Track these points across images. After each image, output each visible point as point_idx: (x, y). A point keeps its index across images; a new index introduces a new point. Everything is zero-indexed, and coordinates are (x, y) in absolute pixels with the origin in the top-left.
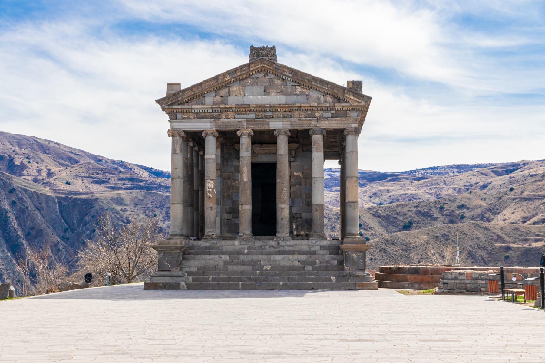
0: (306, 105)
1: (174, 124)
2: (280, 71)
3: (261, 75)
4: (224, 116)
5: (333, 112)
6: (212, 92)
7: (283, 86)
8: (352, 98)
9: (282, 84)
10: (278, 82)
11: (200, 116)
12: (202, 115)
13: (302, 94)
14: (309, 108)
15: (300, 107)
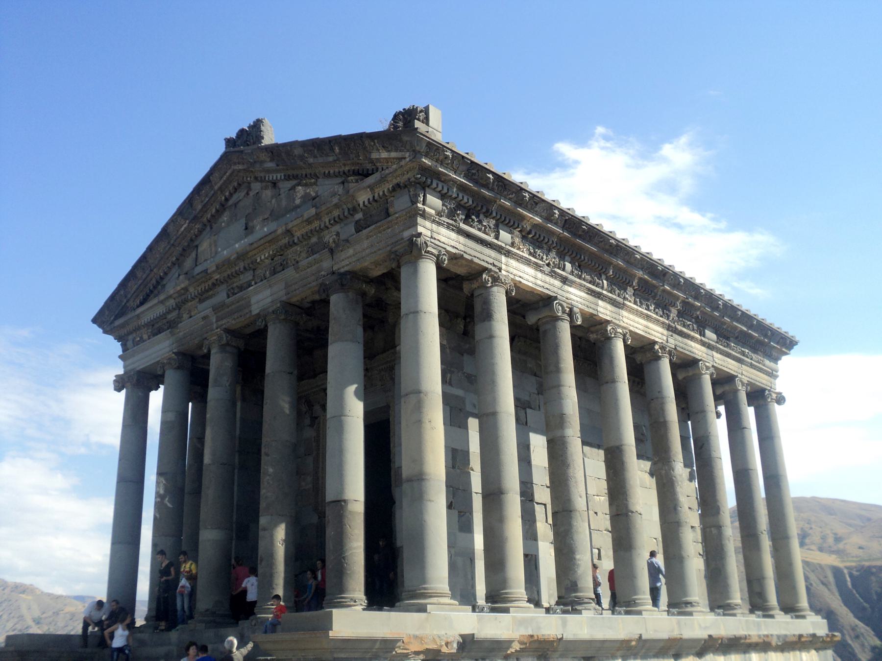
0: (295, 223)
1: (129, 362)
2: (258, 165)
3: (241, 194)
4: (185, 316)
5: (359, 216)
6: (173, 270)
7: (274, 201)
8: (384, 155)
9: (272, 197)
10: (268, 193)
11: (157, 327)
12: (157, 326)
13: (306, 198)
14: (309, 227)
15: (288, 232)
